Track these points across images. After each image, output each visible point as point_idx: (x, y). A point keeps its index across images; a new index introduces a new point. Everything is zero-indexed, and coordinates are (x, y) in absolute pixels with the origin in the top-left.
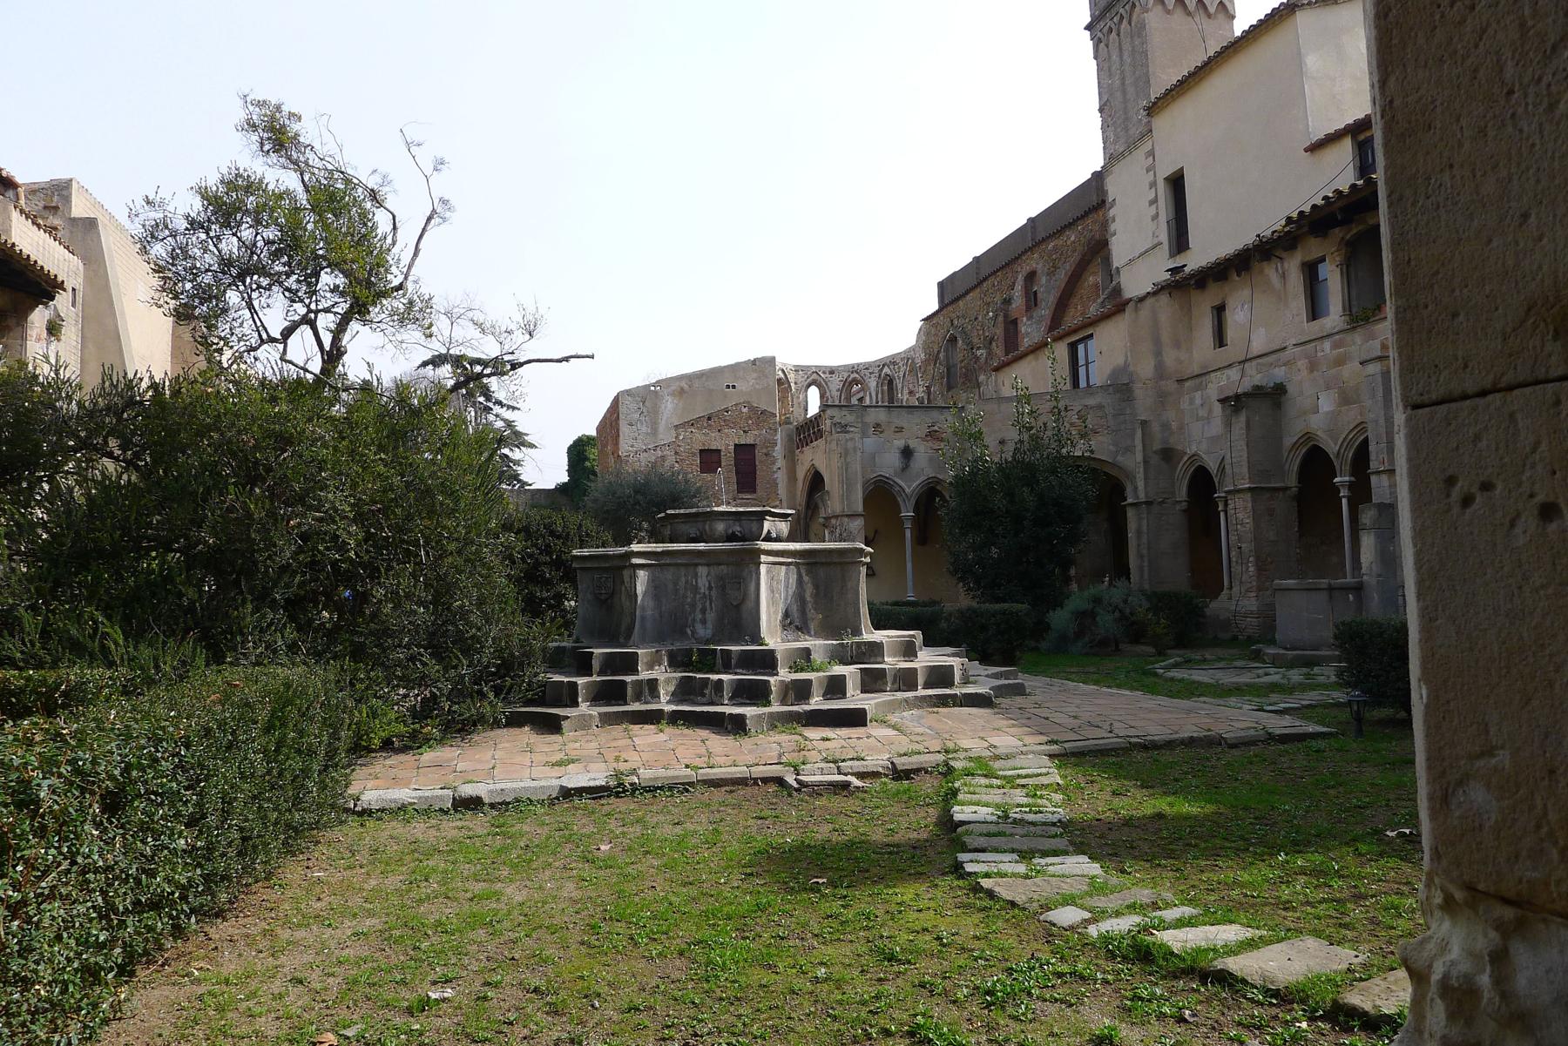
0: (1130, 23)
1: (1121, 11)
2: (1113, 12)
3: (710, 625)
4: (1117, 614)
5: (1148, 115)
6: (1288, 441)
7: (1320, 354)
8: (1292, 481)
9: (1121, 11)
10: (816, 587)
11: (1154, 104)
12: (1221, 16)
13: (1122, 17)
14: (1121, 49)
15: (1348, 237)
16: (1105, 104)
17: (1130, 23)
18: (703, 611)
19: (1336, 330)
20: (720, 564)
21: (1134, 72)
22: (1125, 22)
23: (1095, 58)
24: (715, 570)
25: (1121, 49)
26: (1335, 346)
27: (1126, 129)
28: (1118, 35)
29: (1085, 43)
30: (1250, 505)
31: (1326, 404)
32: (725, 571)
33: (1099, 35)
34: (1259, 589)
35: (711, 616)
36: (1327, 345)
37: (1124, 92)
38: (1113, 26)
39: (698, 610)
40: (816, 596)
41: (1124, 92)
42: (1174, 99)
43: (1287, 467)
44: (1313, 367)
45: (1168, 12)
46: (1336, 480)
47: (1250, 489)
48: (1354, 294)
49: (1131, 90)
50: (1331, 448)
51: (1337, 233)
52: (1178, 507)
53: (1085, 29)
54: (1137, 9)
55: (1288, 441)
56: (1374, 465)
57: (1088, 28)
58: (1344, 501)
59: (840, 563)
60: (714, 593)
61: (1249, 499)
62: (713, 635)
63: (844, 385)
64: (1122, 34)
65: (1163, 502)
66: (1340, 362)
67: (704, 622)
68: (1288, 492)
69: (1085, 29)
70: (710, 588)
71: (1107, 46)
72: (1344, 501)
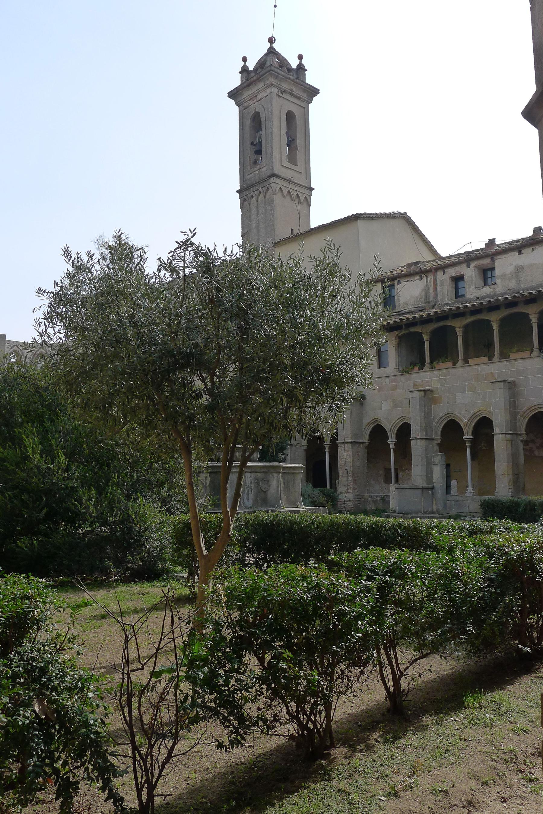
0: (265, 197)
1: (260, 189)
2: (255, 188)
3: (251, 500)
4: (310, 500)
5: (274, 246)
6: (366, 421)
7: (383, 384)
8: (366, 439)
9: (260, 189)
10: (284, 483)
11: (279, 242)
12: (305, 204)
13: (260, 193)
14: (258, 208)
15: (400, 335)
16: (246, 234)
17: (265, 197)
18: (248, 494)
19: (393, 374)
20: (256, 472)
21: (265, 222)
22: (262, 196)
23: (241, 208)
24: (254, 475)
25: (258, 208)
26: (392, 381)
28: (257, 201)
29: (236, 200)
30: (351, 449)
31: (386, 406)
32: (259, 476)
33: (245, 197)
34: (353, 489)
35: (251, 496)
36: (388, 380)
37: (258, 231)
38: (254, 196)
39: (245, 494)
40: (284, 487)
41: (258, 231)
42: (289, 242)
43: (364, 433)
44: (380, 389)
45: (284, 197)
46: (388, 441)
47: (352, 442)
48: (400, 359)
50: (387, 426)
51: (396, 333)
52: (302, 448)
53: (237, 192)
54: (270, 192)
55: (366, 421)
56: (413, 436)
58: (392, 450)
59: (293, 473)
60: (253, 485)
61: (351, 447)
62: (253, 505)
63: (34, 356)
64: (259, 201)
65: (296, 445)
66: (394, 388)
67: (248, 499)
68: (364, 445)
69: (237, 192)
70: (251, 483)
71: (249, 204)
72: (392, 450)
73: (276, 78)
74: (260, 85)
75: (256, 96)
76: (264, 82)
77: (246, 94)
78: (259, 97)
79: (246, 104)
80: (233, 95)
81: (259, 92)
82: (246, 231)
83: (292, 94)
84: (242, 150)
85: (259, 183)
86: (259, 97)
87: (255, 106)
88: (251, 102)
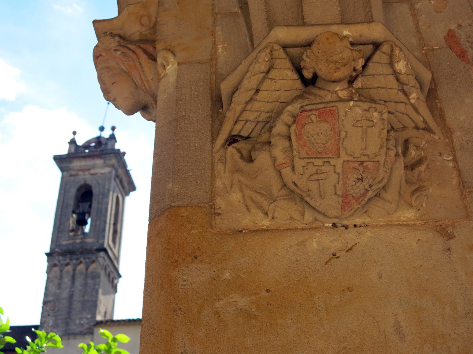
1: (82, 259)
27: (67, 324)
49: (77, 305)
57: (47, 254)
73: (118, 162)
74: (99, 162)
75: (89, 169)
76: (105, 160)
77: (77, 164)
78: (92, 171)
79: (73, 173)
80: (58, 159)
81: (94, 167)
82: (51, 298)
83: (121, 181)
84: (59, 213)
85: (82, 253)
86: (92, 171)
87: (85, 177)
88: (81, 173)
